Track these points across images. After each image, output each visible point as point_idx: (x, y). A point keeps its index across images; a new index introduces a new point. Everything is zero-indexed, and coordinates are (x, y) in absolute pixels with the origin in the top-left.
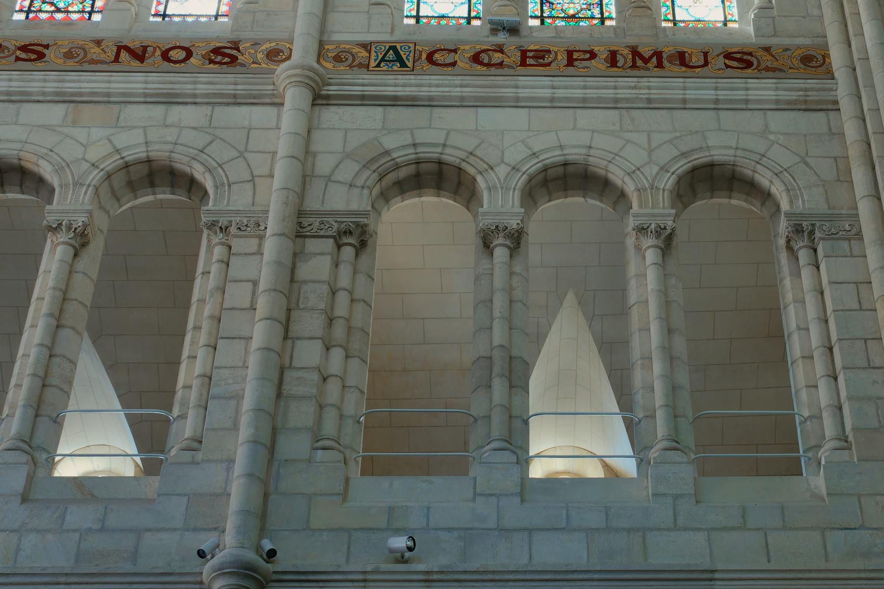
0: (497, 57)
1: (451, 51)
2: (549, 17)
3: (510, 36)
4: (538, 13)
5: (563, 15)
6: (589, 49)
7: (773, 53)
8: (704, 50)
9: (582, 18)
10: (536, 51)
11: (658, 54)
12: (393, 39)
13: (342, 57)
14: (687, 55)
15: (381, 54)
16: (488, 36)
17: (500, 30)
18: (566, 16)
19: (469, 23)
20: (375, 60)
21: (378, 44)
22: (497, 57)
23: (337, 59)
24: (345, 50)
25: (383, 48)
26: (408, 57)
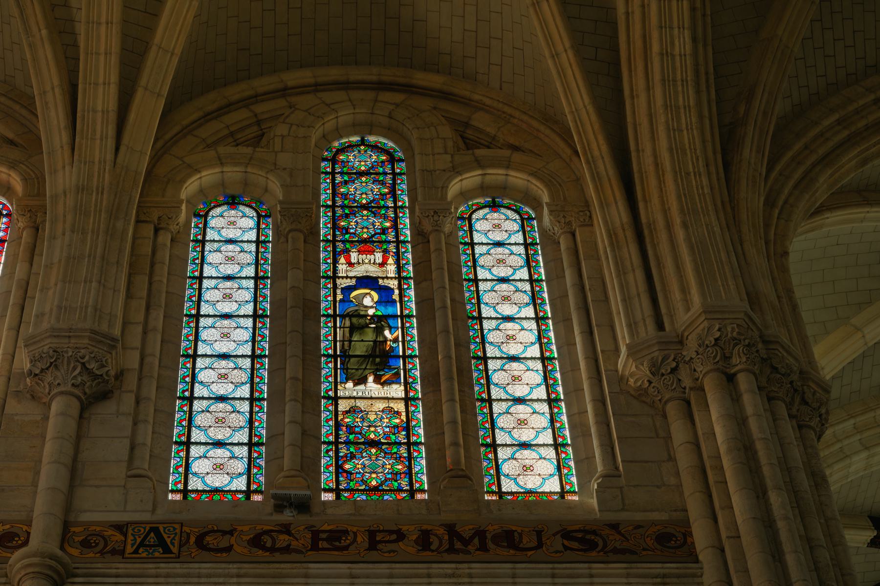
0: (283, 540)
1: (225, 533)
2: (346, 490)
3: (299, 513)
4: (333, 485)
5: (363, 487)
6: (395, 528)
7: (622, 531)
8: (536, 529)
9: (386, 491)
10: (330, 531)
11: (480, 534)
12: (155, 518)
13: (92, 541)
14: (516, 534)
15: (139, 537)
16: (271, 514)
17: (286, 507)
18: (367, 488)
19: (248, 498)
20: (133, 545)
21: (136, 525)
22: (283, 540)
23: (86, 544)
24: (95, 533)
25: (142, 530)
26: (173, 541)
